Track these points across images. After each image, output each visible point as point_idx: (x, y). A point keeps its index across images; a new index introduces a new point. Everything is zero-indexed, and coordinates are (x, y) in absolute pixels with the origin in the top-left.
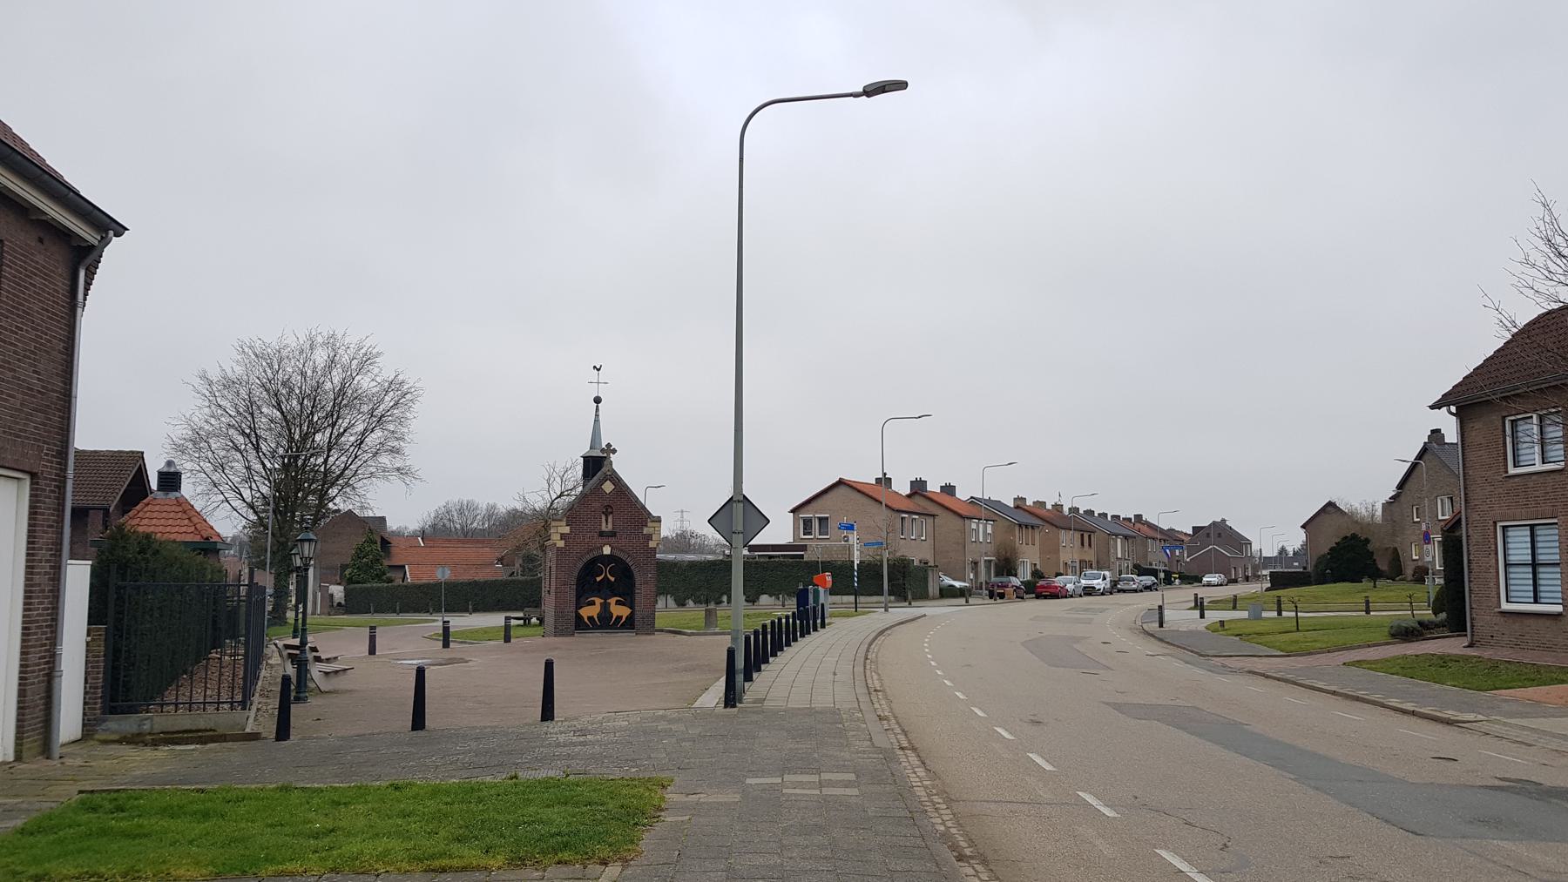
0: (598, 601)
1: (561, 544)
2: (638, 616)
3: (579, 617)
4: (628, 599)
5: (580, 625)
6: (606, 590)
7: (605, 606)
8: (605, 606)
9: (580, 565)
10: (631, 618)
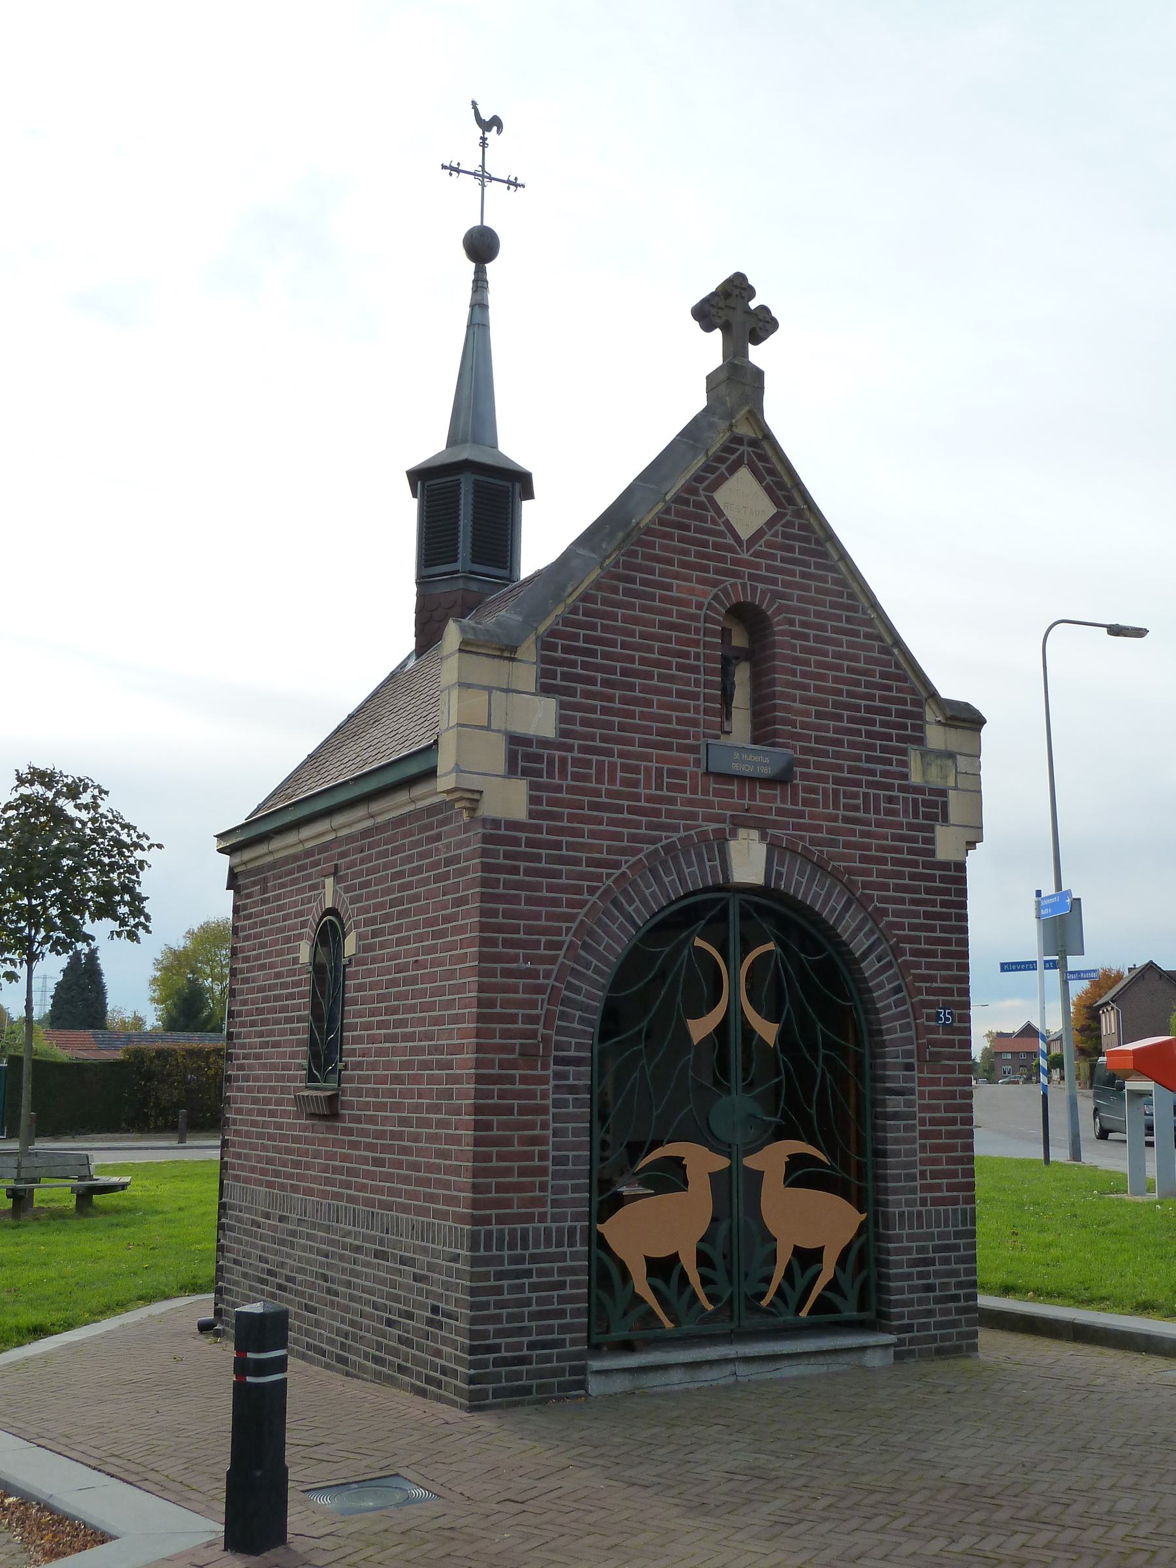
0: (701, 1162)
1: (510, 800)
2: (903, 1247)
3: (606, 1271)
4: (845, 1161)
5: (617, 1312)
7: (736, 1193)
8: (736, 1193)
10: (864, 1255)
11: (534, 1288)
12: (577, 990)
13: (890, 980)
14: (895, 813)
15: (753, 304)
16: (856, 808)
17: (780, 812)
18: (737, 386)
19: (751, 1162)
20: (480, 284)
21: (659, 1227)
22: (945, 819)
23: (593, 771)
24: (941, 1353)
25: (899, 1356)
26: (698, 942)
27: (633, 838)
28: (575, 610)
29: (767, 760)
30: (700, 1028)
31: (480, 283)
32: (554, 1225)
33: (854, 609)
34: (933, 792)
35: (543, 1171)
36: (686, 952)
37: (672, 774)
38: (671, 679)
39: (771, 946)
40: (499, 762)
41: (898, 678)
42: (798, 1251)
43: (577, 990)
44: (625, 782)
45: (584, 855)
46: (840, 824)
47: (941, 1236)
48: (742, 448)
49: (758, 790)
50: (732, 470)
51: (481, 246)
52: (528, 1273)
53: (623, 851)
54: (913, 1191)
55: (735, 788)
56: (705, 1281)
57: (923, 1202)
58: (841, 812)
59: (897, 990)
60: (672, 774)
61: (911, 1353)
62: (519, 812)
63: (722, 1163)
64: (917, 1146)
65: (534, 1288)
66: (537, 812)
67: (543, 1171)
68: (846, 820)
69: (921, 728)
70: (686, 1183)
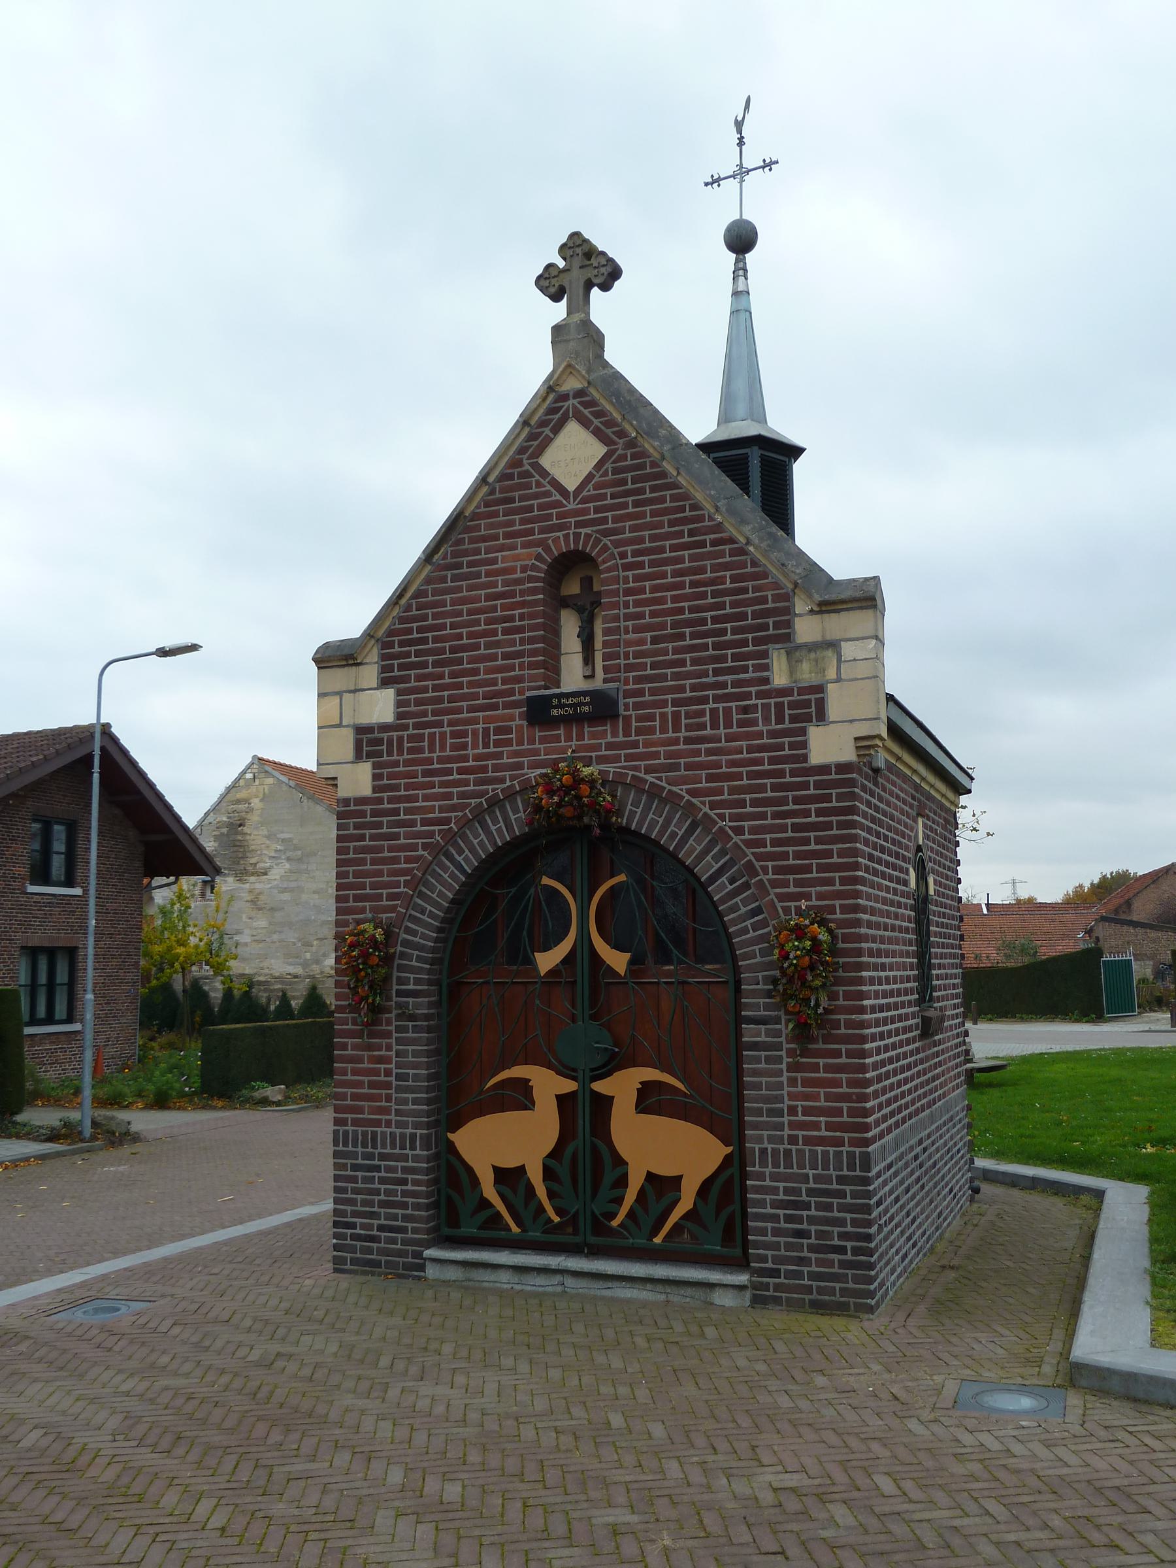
0: (547, 1084)
1: (359, 780)
3: (452, 1173)
5: (459, 1210)
6: (597, 1025)
7: (585, 1117)
8: (585, 1117)
9: (445, 886)
10: (726, 1189)
11: (382, 1181)
12: (414, 933)
13: (745, 902)
14: (754, 722)
15: (561, 264)
16: (702, 726)
17: (610, 746)
18: (578, 342)
19: (599, 1086)
20: (741, 273)
21: (510, 1142)
22: (821, 716)
23: (426, 743)
24: (818, 1307)
25: (757, 1301)
26: (546, 881)
27: (462, 795)
28: (408, 608)
29: (588, 699)
30: (547, 961)
31: (740, 270)
32: (398, 1131)
33: (700, 519)
34: (802, 690)
35: (388, 1086)
36: (532, 891)
37: (498, 731)
38: (497, 644)
39: (622, 878)
40: (349, 752)
41: (754, 577)
42: (651, 1177)
43: (414, 933)
44: (454, 747)
45: (418, 817)
46: (682, 747)
47: (817, 1179)
48: (566, 404)
49: (586, 729)
50: (557, 429)
51: (741, 240)
52: (377, 1169)
53: (454, 808)
54: (780, 1127)
55: (561, 732)
56: (551, 1195)
57: (793, 1140)
58: (683, 734)
59: (757, 911)
60: (498, 731)
61: (777, 1301)
62: (366, 790)
63: (569, 1086)
64: (784, 1079)
65: (382, 1181)
66: (378, 786)
67: (388, 1086)
68: (688, 741)
69: (789, 624)
70: (533, 1103)
